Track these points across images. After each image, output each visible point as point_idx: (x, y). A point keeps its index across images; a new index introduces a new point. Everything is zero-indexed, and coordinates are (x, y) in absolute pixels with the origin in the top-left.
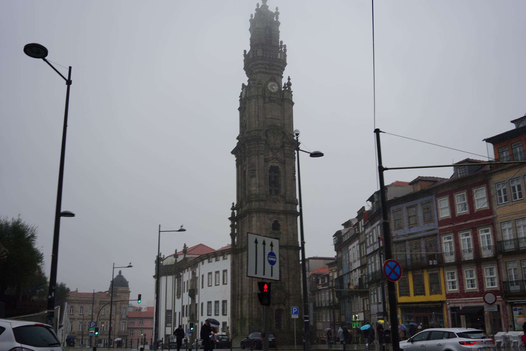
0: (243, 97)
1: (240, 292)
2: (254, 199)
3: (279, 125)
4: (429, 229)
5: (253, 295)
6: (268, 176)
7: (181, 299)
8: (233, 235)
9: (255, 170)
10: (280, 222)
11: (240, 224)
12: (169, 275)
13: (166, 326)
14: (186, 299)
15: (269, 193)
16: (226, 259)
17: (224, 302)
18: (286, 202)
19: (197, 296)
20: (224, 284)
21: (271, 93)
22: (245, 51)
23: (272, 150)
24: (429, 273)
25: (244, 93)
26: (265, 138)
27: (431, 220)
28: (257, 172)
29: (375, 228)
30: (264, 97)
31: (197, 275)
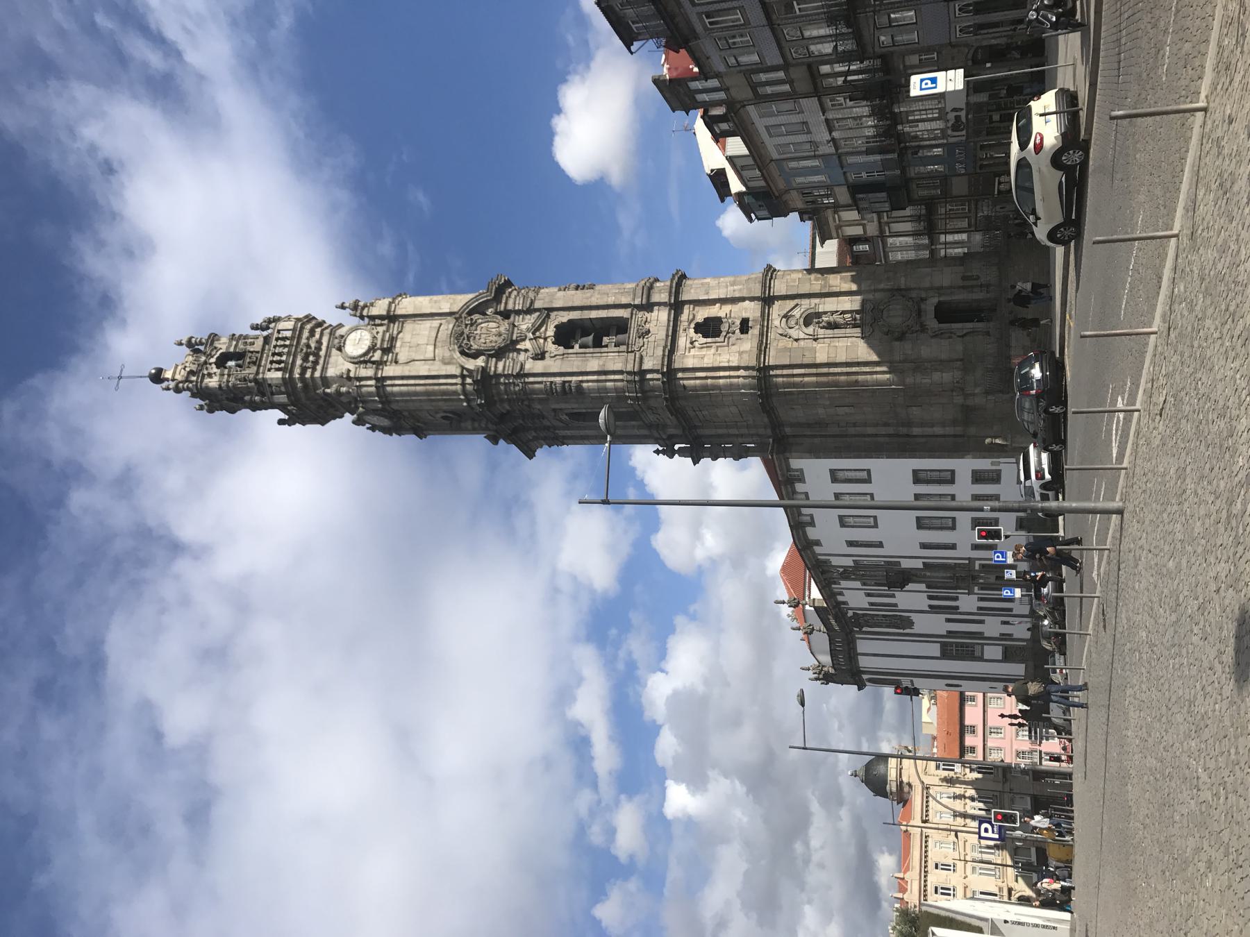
0: (386, 422)
1: (891, 430)
3: (451, 326)
7: (914, 616)
8: (739, 453)
11: (707, 432)
12: (855, 648)
13: (981, 659)
14: (911, 598)
15: (623, 348)
16: (801, 471)
17: (918, 477)
18: (648, 307)
19: (905, 564)
20: (868, 480)
22: (281, 422)
25: (376, 420)
26: (482, 358)
29: (699, 14)
30: (379, 364)
31: (849, 562)
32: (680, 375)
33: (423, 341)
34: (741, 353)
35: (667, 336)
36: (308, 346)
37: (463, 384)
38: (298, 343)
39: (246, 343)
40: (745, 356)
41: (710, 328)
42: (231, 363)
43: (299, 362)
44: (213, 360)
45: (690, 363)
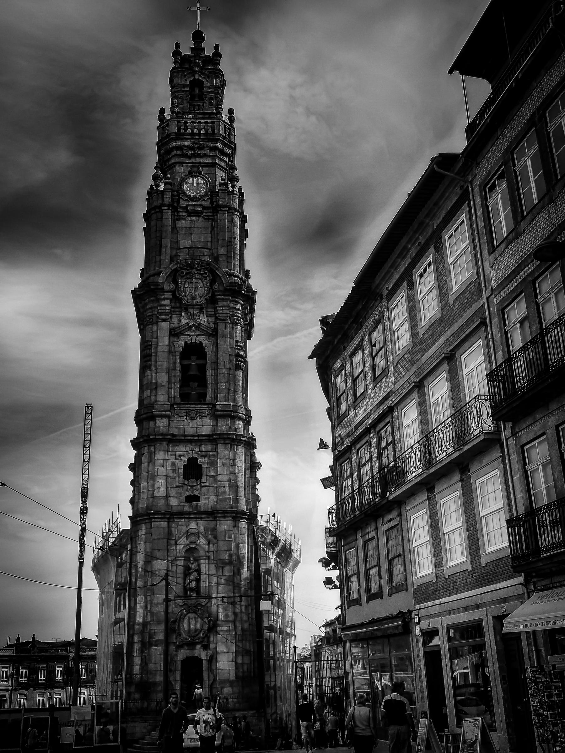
2: (145, 416)
4: (381, 398)
5: (137, 627)
6: (178, 366)
9: (150, 355)
10: (201, 461)
15: (178, 400)
17: (121, 646)
18: (216, 417)
21: (192, 199)
23: (186, 309)
24: (386, 527)
26: (172, 286)
27: (385, 372)
28: (153, 358)
30: (174, 207)
32: (152, 449)
33: (195, 237)
34: (167, 498)
35: (185, 436)
36: (201, 148)
37: (154, 275)
38: (203, 140)
39: (211, 99)
40: (162, 502)
41: (193, 471)
42: (197, 91)
43: (186, 143)
44: (197, 77)
45: (160, 457)
